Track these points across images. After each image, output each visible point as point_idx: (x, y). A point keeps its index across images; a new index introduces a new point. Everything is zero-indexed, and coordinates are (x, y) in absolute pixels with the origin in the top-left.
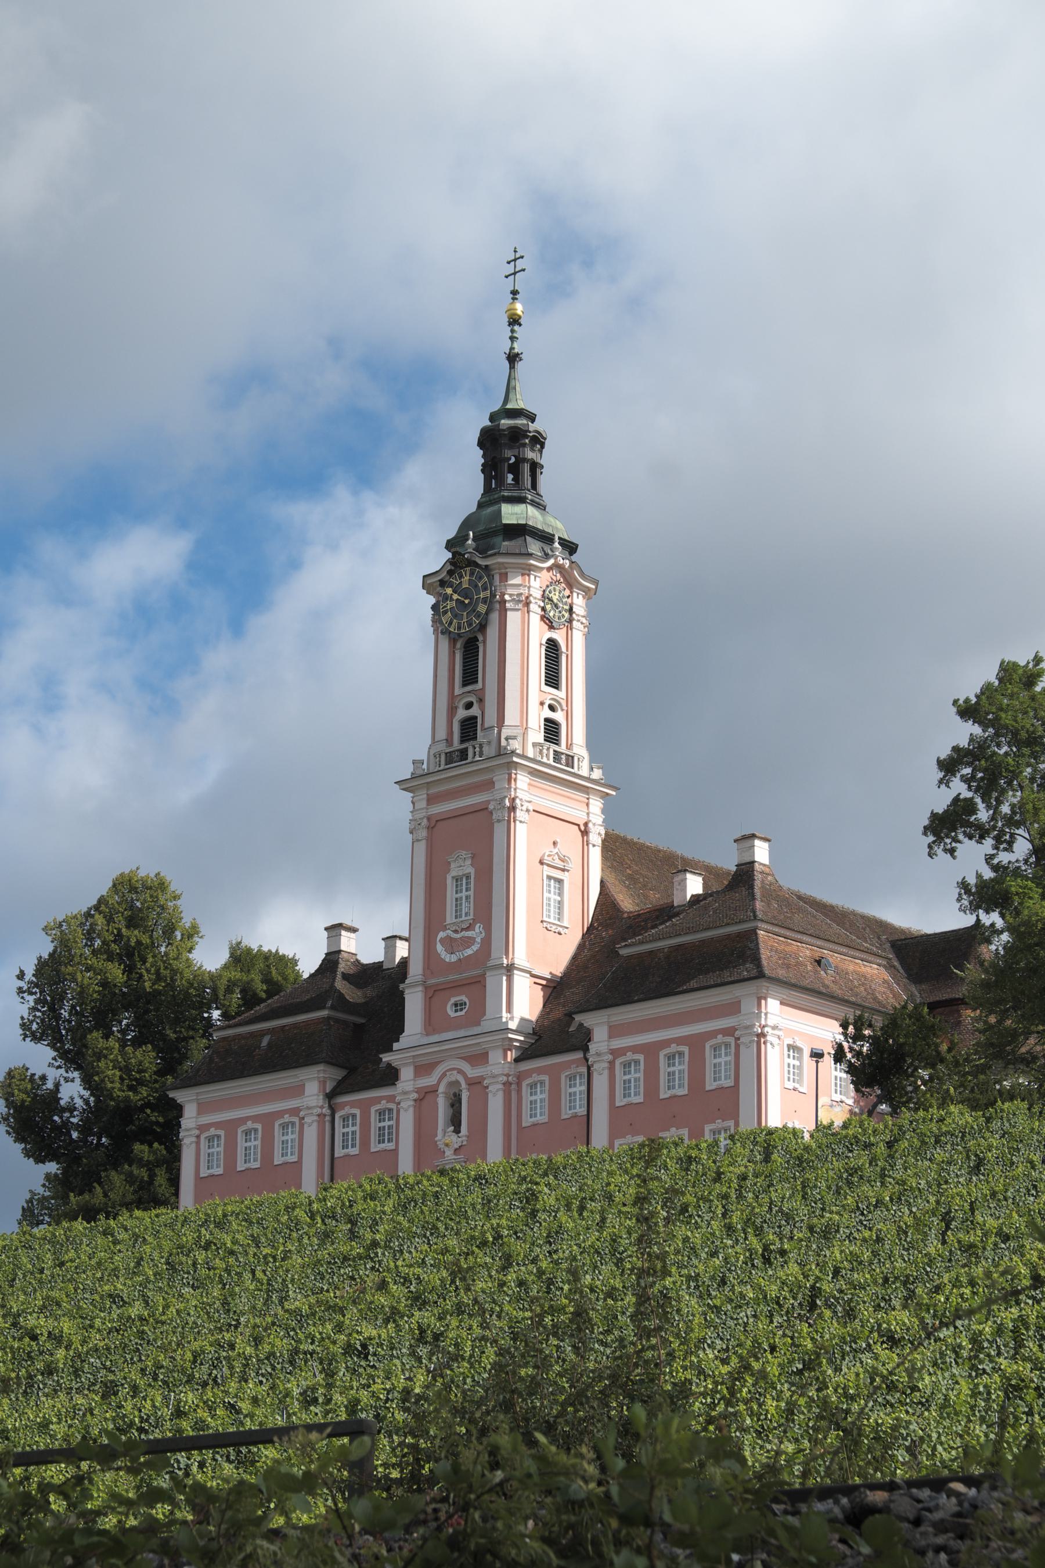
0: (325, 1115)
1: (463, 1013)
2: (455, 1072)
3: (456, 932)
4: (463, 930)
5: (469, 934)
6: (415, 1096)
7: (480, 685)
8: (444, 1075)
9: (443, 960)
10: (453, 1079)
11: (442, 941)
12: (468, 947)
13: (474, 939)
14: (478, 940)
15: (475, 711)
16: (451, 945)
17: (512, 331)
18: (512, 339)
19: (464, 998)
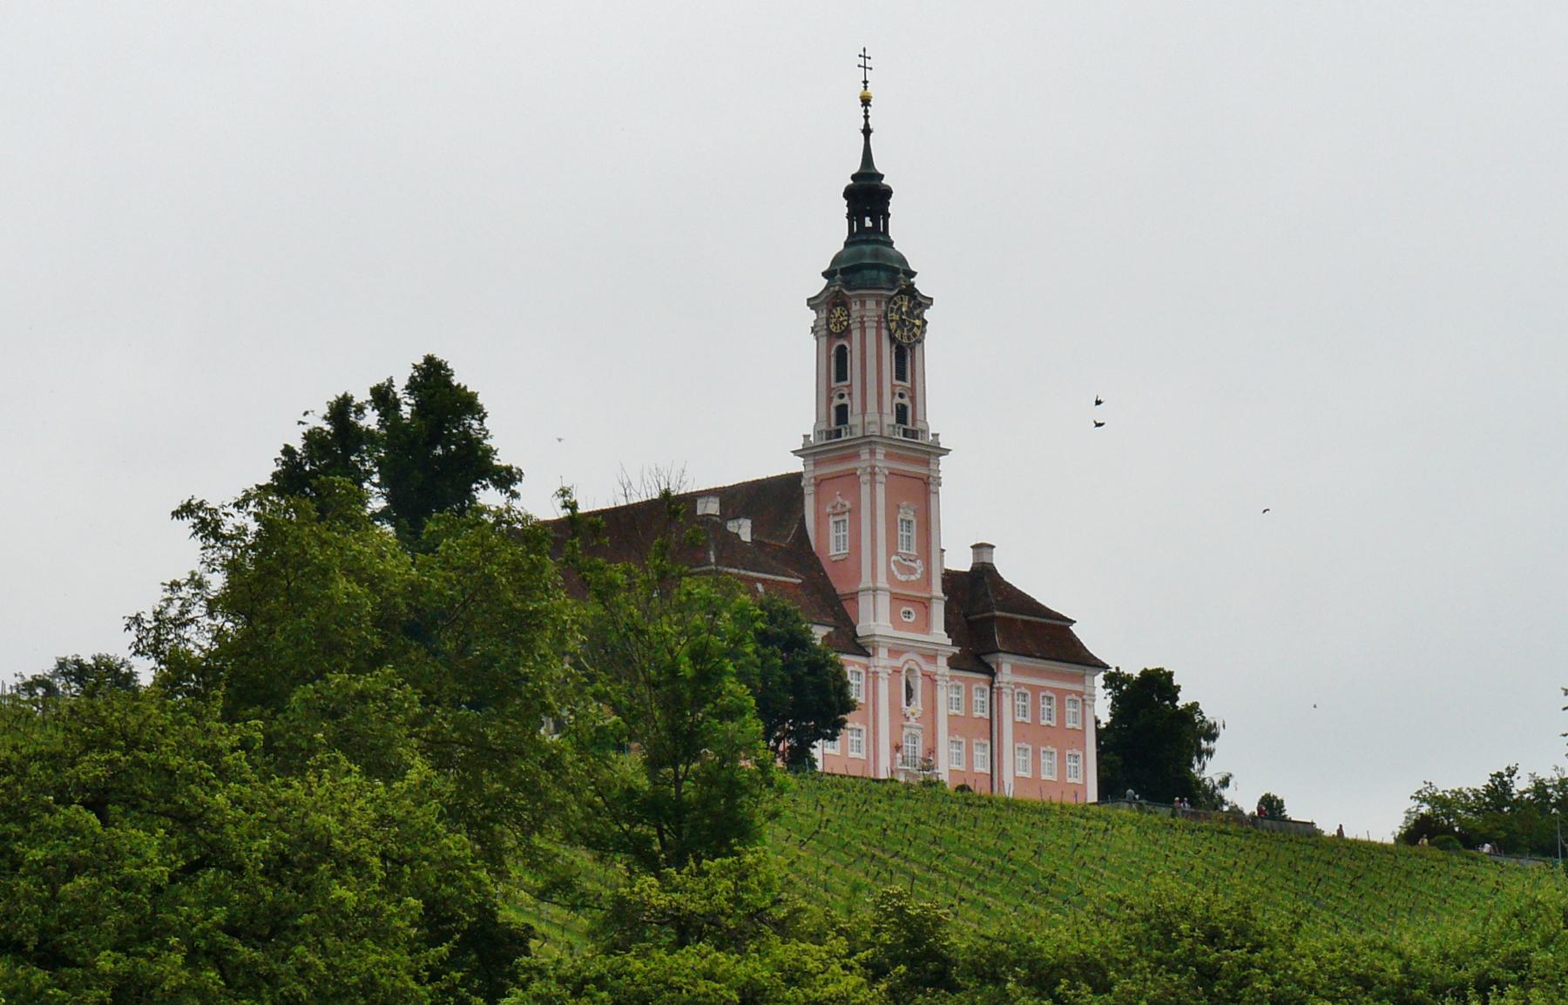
3: (905, 560)
7: (908, 384)
8: (906, 662)
9: (896, 577)
14: (919, 571)
15: (906, 401)
17: (866, 111)
18: (866, 117)
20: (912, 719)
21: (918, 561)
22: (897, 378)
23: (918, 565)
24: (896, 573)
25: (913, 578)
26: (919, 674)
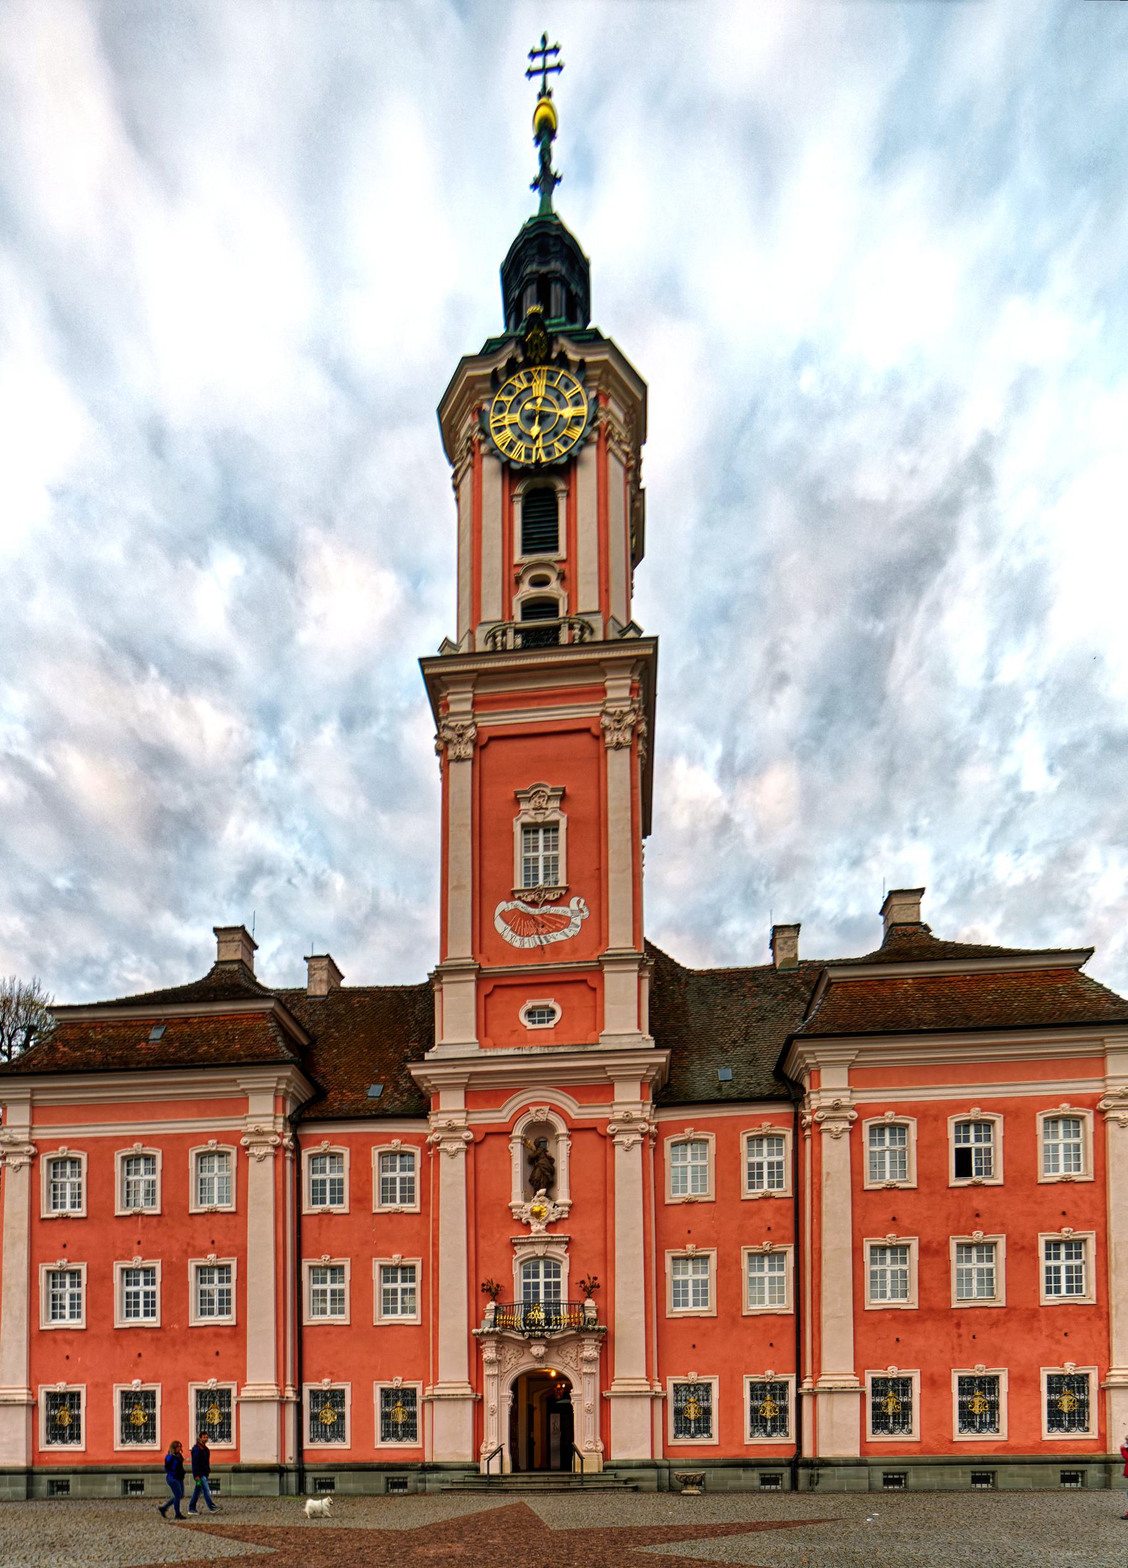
0: (286, 1149)
1: (551, 1024)
2: (546, 1108)
3: (533, 904)
4: (547, 902)
5: (559, 910)
6: (469, 1135)
7: (562, 553)
8: (525, 1110)
10: (542, 1117)
11: (503, 915)
12: (558, 930)
13: (566, 921)
15: (554, 589)
16: (519, 922)
19: (552, 1003)
20: (537, 1227)
21: (573, 902)
22: (525, 551)
23: (576, 909)
24: (508, 936)
25: (559, 937)
26: (562, 1129)
